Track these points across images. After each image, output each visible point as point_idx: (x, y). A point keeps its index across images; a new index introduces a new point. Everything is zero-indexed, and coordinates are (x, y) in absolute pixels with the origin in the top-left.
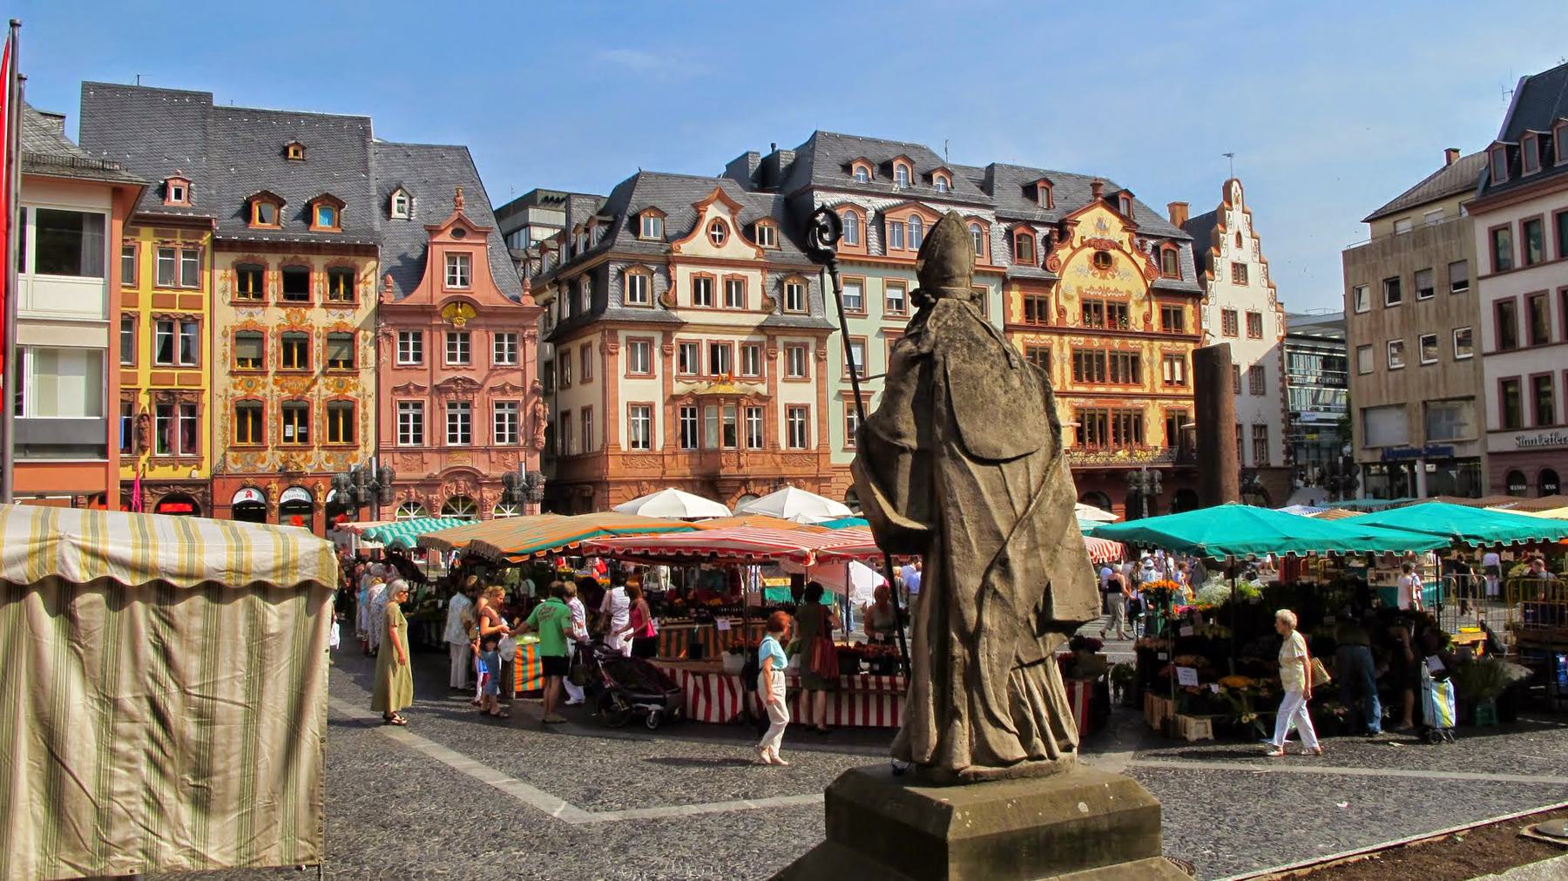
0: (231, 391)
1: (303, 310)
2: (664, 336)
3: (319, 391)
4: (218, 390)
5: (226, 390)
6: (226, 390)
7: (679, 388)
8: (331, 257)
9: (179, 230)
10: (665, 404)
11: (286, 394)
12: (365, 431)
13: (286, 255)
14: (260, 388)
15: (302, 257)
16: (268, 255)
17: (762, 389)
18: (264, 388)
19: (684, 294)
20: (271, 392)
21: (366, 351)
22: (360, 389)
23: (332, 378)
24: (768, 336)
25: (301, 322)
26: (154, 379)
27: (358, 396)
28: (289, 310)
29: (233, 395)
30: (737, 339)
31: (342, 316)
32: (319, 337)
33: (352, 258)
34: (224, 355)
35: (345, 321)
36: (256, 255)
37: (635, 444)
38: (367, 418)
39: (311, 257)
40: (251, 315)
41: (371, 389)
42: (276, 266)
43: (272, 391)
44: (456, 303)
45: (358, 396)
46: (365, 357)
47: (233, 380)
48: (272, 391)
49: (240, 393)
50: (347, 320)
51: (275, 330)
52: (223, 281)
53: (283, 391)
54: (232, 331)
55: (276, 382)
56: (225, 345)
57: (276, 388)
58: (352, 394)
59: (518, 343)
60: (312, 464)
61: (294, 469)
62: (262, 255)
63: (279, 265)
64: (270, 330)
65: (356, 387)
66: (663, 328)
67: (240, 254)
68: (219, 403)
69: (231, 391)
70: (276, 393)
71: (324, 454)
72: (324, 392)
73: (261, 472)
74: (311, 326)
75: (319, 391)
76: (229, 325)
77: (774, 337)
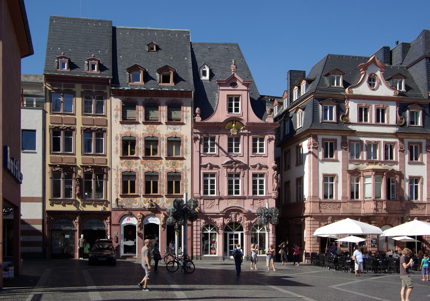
0: (120, 167)
1: (155, 126)
2: (342, 139)
3: (163, 167)
4: (114, 166)
5: (117, 167)
6: (117, 167)
7: (352, 167)
8: (169, 98)
9: (94, 85)
10: (343, 176)
11: (147, 169)
12: (186, 188)
13: (146, 98)
14: (134, 166)
15: (155, 98)
16: (138, 98)
17: (397, 168)
18: (136, 166)
19: (353, 116)
21: (187, 145)
22: (184, 167)
23: (170, 161)
25: (154, 132)
27: (183, 170)
28: (148, 126)
29: (121, 169)
30: (382, 140)
31: (174, 129)
32: (163, 140)
33: (180, 99)
34: (116, 149)
35: (176, 131)
36: (132, 97)
37: (325, 197)
38: (187, 181)
39: (159, 98)
40: (130, 128)
41: (189, 167)
42: (142, 103)
43: (140, 167)
44: (233, 121)
45: (183, 170)
46: (186, 150)
47: (121, 161)
48: (140, 167)
49: (125, 168)
50: (177, 131)
51: (142, 136)
52: (116, 111)
53: (145, 167)
54: (120, 136)
55: (142, 163)
56: (117, 144)
57: (142, 166)
58: (179, 169)
59: (265, 143)
62: (135, 98)
63: (143, 102)
65: (181, 165)
66: (342, 134)
69: (120, 167)
70: (142, 168)
72: (166, 168)
73: (135, 208)
74: (159, 134)
75: (163, 167)
76: (118, 133)
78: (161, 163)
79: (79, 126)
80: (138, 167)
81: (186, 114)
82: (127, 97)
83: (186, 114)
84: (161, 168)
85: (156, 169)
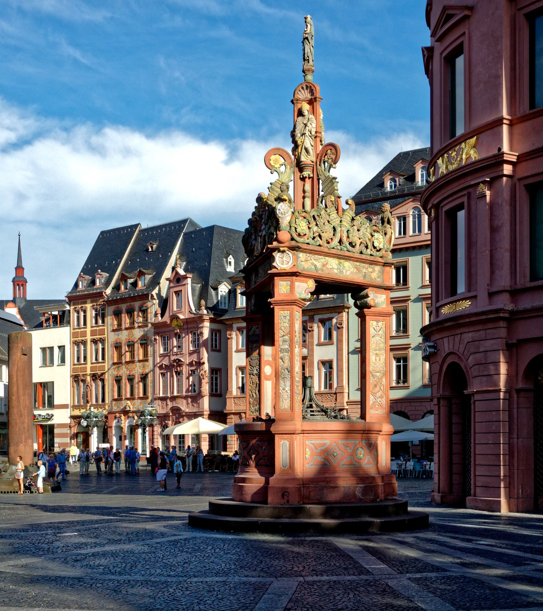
1: (133, 330)
20: (124, 372)
23: (141, 363)
24: (309, 316)
25: (132, 336)
26: (92, 369)
28: (128, 331)
36: (119, 305)
53: (127, 371)
57: (125, 370)
60: (135, 406)
61: (128, 409)
62: (121, 305)
64: (123, 342)
67: (115, 306)
68: (110, 378)
70: (125, 372)
71: (139, 401)
74: (135, 338)
77: (313, 316)
78: (136, 366)
79: (89, 338)
80: (123, 372)
81: (151, 316)
82: (116, 306)
83: (151, 316)
84: (136, 371)
85: (133, 372)
